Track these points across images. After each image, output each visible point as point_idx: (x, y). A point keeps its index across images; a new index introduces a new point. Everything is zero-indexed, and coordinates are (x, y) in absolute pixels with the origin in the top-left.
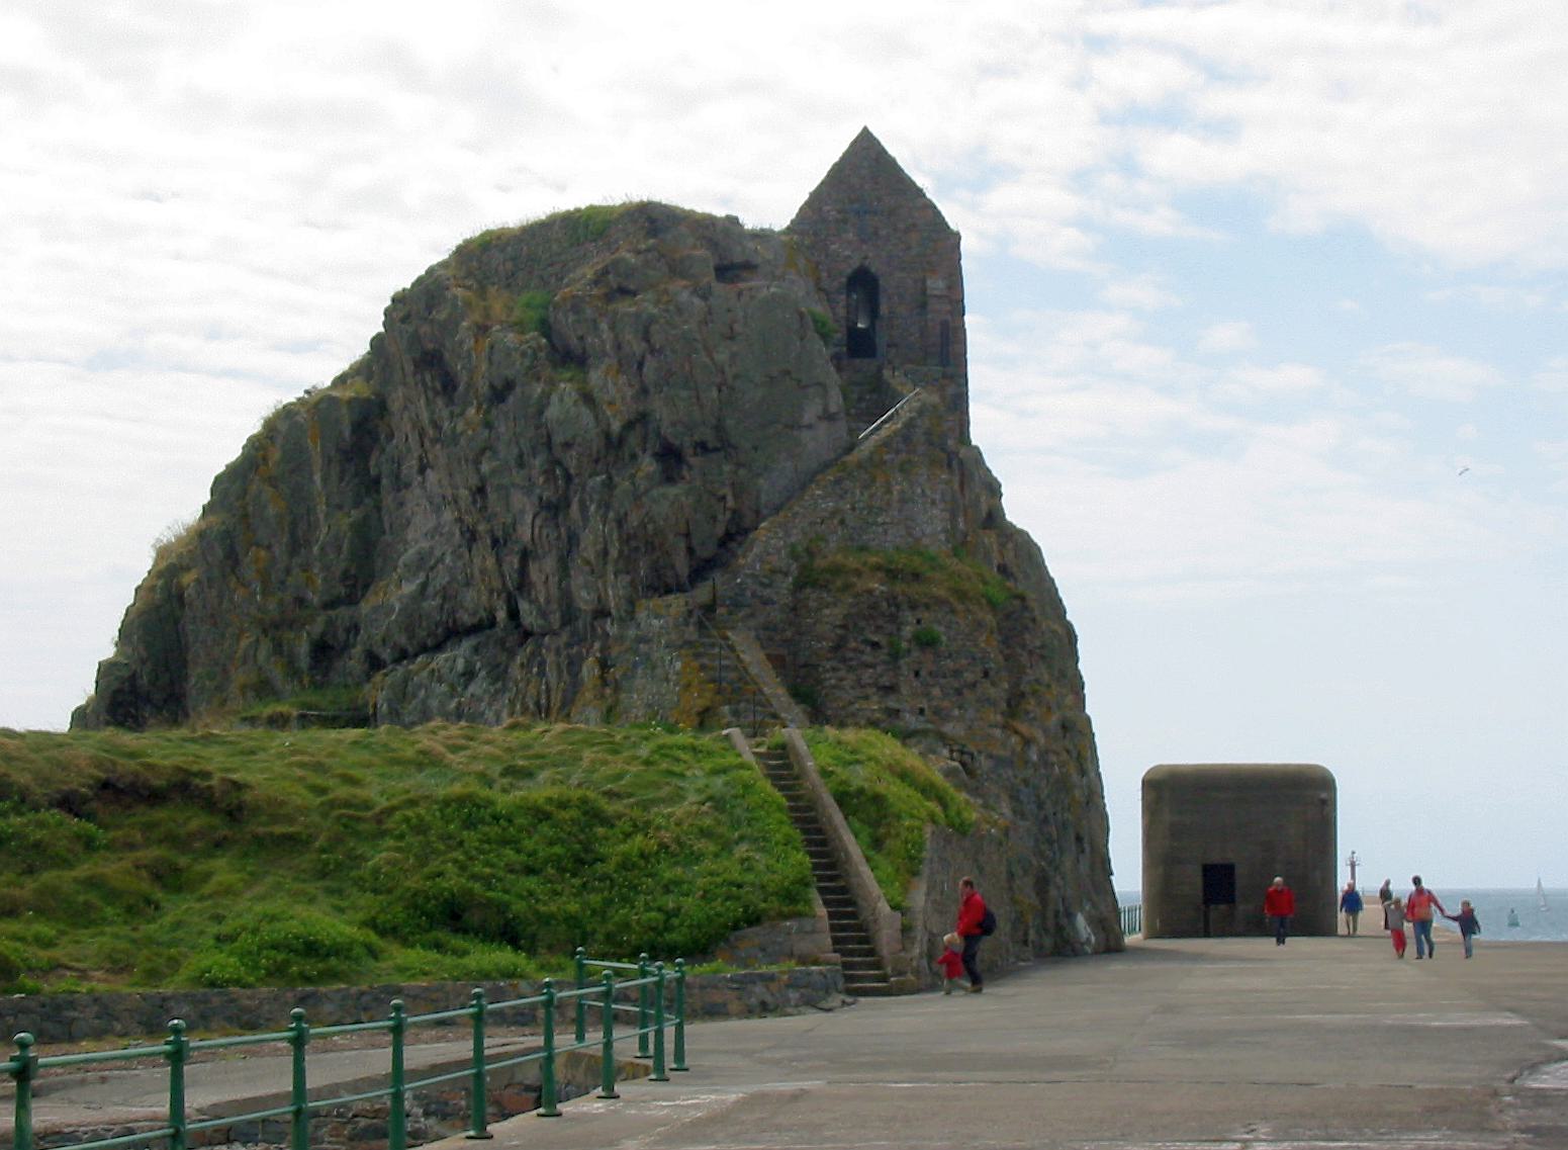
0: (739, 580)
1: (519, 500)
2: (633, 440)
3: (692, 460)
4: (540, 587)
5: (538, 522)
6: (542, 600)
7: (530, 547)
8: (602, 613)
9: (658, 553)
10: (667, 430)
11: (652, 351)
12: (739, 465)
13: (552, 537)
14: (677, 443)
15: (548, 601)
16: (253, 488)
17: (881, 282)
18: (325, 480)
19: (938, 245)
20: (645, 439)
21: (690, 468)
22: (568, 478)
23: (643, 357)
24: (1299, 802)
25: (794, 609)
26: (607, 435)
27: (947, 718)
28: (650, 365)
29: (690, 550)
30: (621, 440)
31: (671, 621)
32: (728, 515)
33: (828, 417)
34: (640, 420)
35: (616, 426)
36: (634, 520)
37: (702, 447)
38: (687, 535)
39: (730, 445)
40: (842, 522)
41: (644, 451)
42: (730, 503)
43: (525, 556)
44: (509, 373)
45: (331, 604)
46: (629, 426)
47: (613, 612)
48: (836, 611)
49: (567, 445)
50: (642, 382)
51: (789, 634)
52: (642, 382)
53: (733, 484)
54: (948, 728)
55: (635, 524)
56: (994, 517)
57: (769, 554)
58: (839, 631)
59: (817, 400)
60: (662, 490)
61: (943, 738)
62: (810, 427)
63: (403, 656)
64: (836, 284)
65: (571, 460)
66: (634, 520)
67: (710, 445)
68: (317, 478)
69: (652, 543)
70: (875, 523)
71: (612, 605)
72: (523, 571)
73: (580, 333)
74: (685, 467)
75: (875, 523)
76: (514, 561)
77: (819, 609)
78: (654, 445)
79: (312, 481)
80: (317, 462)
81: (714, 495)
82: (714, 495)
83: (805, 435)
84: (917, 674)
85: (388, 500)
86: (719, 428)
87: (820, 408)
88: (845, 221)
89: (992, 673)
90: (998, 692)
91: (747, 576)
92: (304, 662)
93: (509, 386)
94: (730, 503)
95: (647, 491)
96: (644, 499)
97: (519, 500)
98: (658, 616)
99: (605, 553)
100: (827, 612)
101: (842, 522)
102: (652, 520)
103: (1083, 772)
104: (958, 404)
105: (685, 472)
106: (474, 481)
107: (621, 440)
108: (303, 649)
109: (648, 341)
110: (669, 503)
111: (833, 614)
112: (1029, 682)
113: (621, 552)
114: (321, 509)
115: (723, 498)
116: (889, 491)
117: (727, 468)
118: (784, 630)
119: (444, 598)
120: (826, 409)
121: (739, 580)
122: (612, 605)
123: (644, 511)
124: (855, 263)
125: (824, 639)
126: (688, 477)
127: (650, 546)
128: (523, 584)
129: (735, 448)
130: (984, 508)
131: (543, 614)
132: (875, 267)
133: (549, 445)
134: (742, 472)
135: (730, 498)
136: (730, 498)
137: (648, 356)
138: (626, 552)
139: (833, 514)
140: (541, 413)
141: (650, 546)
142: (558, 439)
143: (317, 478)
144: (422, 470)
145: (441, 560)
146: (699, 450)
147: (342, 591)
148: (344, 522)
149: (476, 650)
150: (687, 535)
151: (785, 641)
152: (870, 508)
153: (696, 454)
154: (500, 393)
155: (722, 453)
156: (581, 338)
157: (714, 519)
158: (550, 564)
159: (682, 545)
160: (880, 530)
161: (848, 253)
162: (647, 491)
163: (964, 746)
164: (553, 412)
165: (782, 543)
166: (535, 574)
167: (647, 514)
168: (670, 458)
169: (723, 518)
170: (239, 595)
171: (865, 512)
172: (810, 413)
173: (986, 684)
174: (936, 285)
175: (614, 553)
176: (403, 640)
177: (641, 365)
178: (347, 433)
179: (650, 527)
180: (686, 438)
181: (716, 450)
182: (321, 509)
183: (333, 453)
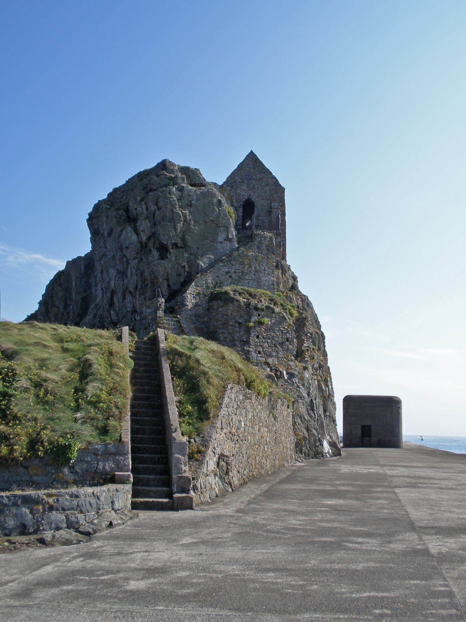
2: (150, 244)
3: (171, 251)
4: (117, 304)
5: (117, 279)
6: (117, 309)
7: (114, 289)
11: (159, 209)
12: (191, 254)
13: (121, 285)
14: (165, 243)
15: (119, 310)
16: (55, 288)
17: (255, 204)
18: (76, 284)
19: (277, 192)
20: (154, 243)
21: (170, 253)
23: (155, 211)
24: (389, 407)
25: (208, 310)
26: (141, 243)
27: (270, 356)
29: (169, 286)
30: (146, 244)
32: (186, 274)
35: (144, 239)
37: (175, 245)
38: (168, 280)
39: (187, 246)
41: (154, 248)
42: (187, 269)
46: (149, 239)
47: (138, 310)
49: (127, 248)
50: (154, 221)
51: (206, 319)
52: (154, 221)
54: (270, 360)
56: (294, 288)
57: (198, 286)
60: (159, 261)
61: (267, 364)
62: (221, 243)
64: (239, 204)
65: (127, 253)
67: (179, 245)
68: (74, 284)
70: (245, 279)
71: (138, 307)
72: (112, 299)
73: (135, 207)
75: (245, 279)
76: (109, 294)
77: (218, 309)
78: (157, 245)
79: (72, 285)
80: (74, 278)
83: (219, 246)
84: (258, 337)
86: (183, 239)
87: (226, 236)
88: (243, 182)
89: (290, 339)
90: (293, 347)
91: (189, 293)
94: (187, 269)
98: (149, 308)
99: (137, 287)
100: (220, 309)
101: (230, 277)
103: (327, 386)
104: (282, 244)
105: (168, 255)
107: (146, 244)
109: (157, 206)
112: (305, 347)
113: (141, 286)
115: (184, 267)
116: (250, 267)
117: (186, 255)
118: (203, 317)
119: (101, 318)
122: (138, 307)
123: (150, 270)
124: (246, 197)
129: (189, 247)
130: (291, 284)
131: (117, 314)
132: (254, 198)
133: (121, 249)
134: (192, 257)
135: (187, 267)
136: (187, 267)
137: (157, 211)
138: (143, 286)
139: (228, 273)
142: (124, 246)
143: (74, 284)
146: (174, 247)
150: (168, 280)
151: (204, 322)
152: (243, 272)
153: (173, 248)
155: (184, 249)
156: (136, 209)
157: (180, 275)
158: (120, 295)
159: (166, 283)
160: (246, 281)
161: (244, 193)
163: (277, 367)
169: (184, 275)
172: (221, 238)
173: (287, 343)
174: (275, 204)
175: (139, 287)
177: (154, 214)
178: (83, 268)
179: (153, 276)
181: (181, 247)
183: (78, 275)
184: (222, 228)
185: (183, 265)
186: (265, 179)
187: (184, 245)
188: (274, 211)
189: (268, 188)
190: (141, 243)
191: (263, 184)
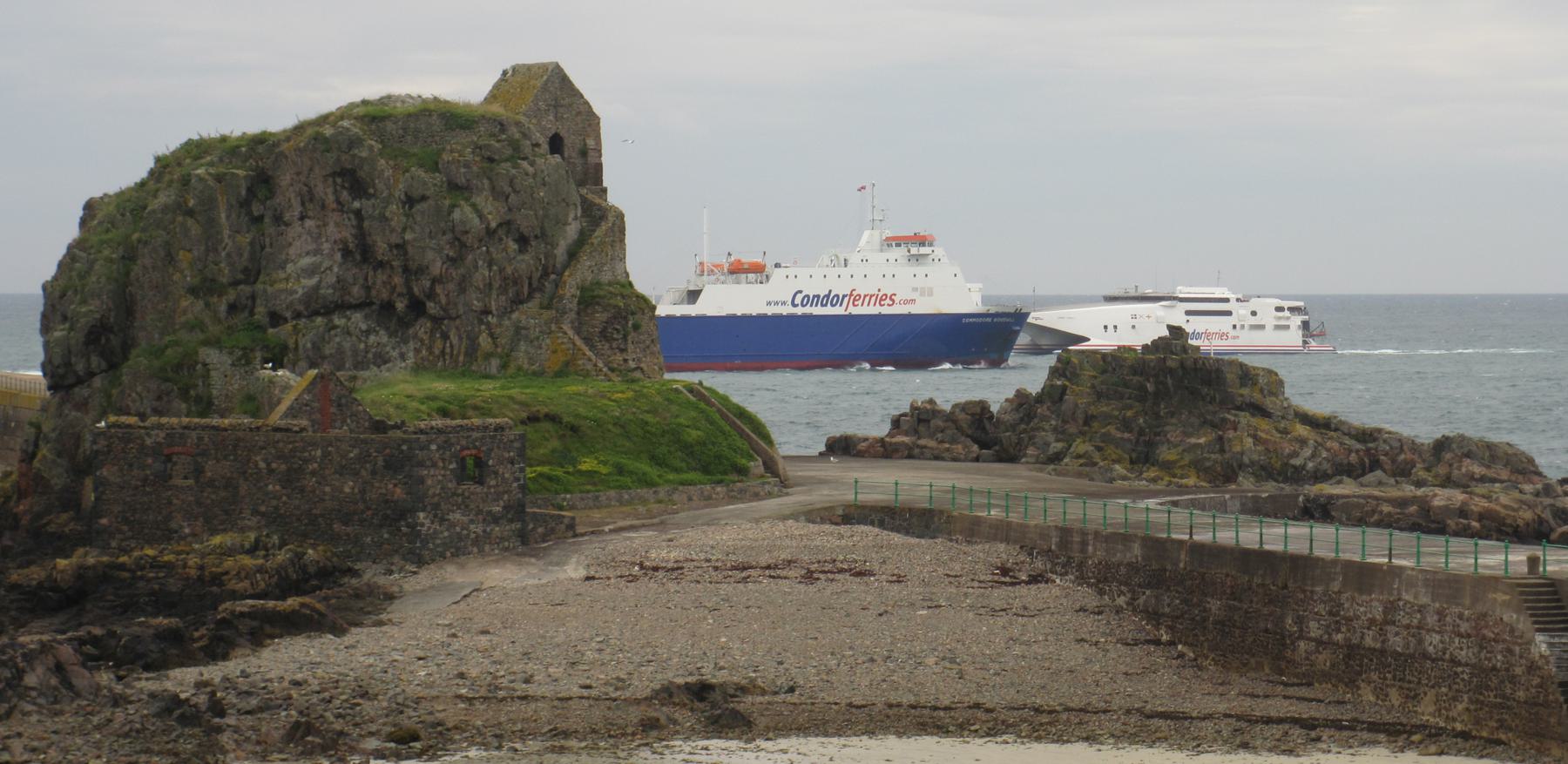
1: (430, 255)
2: (500, 232)
8: (487, 312)
18: (228, 217)
19: (589, 121)
20: (508, 232)
22: (463, 245)
28: (513, 197)
33: (576, 218)
34: (506, 224)
35: (493, 225)
36: (509, 270)
43: (434, 281)
44: (428, 193)
45: (235, 283)
46: (500, 225)
63: (298, 315)
66: (509, 270)
68: (223, 215)
85: (270, 230)
86: (542, 228)
92: (223, 315)
93: (424, 198)
97: (430, 255)
106: (395, 239)
107: (495, 231)
108: (223, 308)
110: (525, 263)
114: (226, 232)
128: (431, 295)
132: (563, 133)
133: (453, 231)
140: (450, 213)
141: (515, 283)
143: (223, 215)
144: (302, 218)
145: (330, 268)
147: (241, 276)
148: (245, 239)
149: (366, 317)
154: (410, 201)
164: (456, 215)
166: (439, 289)
168: (523, 241)
170: (176, 277)
174: (591, 143)
175: (496, 285)
176: (301, 308)
178: (244, 192)
182: (226, 232)
188: (591, 153)
190: (487, 228)
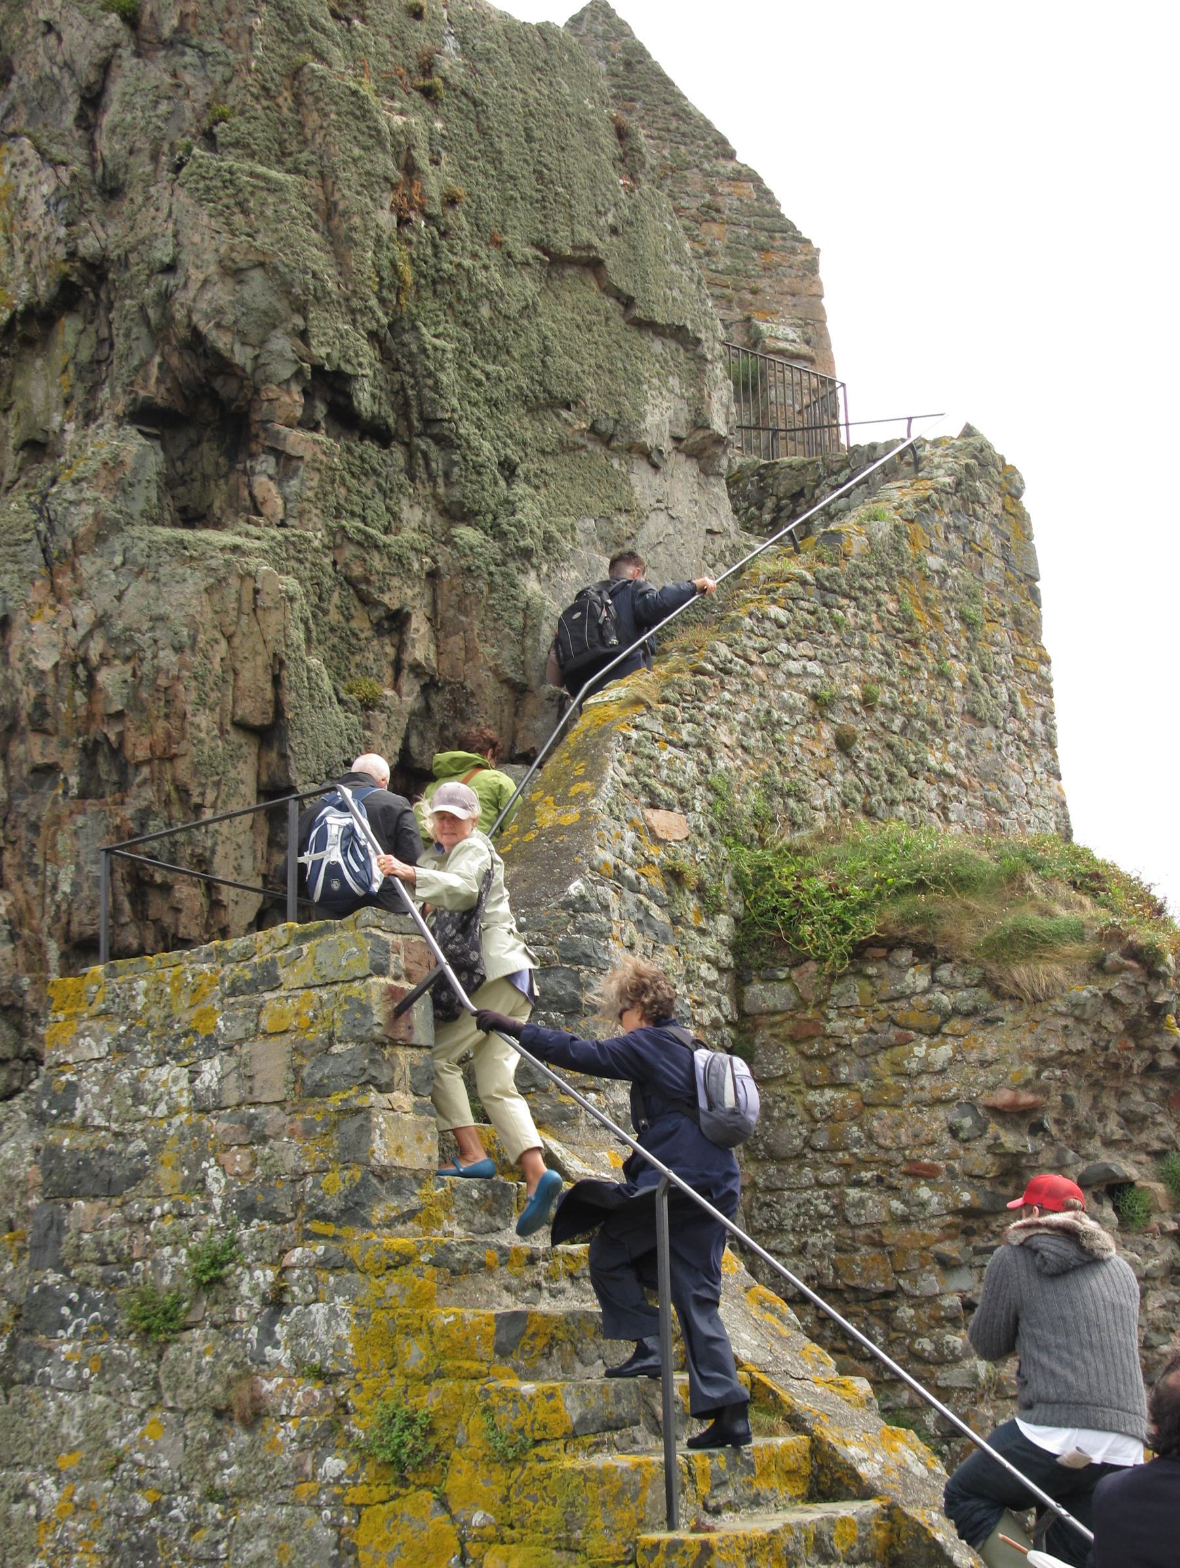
0: (576, 887)
9: (142, 796)
10: (204, 299)
21: (286, 462)
31: (272, 1065)
40: (844, 743)
48: (990, 1044)
53: (433, 575)
55: (45, 663)
58: (1010, 1140)
59: (674, 382)
67: (365, 399)
69: (116, 752)
74: (266, 465)
81: (365, 600)
82: (365, 600)
87: (685, 415)
94: (421, 650)
95: (104, 530)
96: (88, 566)
102: (124, 647)
105: (264, 486)
111: (997, 1057)
115: (397, 621)
120: (699, 423)
121: (576, 887)
123: (84, 613)
125: (921, 1173)
126: (276, 506)
127: (105, 763)
129: (445, 442)
135: (419, 625)
146: (321, 410)
155: (398, 455)
162: (104, 530)
165: (692, 769)
167: (101, 622)
171: (896, 726)
174: (781, 332)
180: (281, 343)
184: (657, 346)
185: (391, 600)
186: (693, 175)
187: (403, 410)
189: (715, 234)
191: (693, 205)
